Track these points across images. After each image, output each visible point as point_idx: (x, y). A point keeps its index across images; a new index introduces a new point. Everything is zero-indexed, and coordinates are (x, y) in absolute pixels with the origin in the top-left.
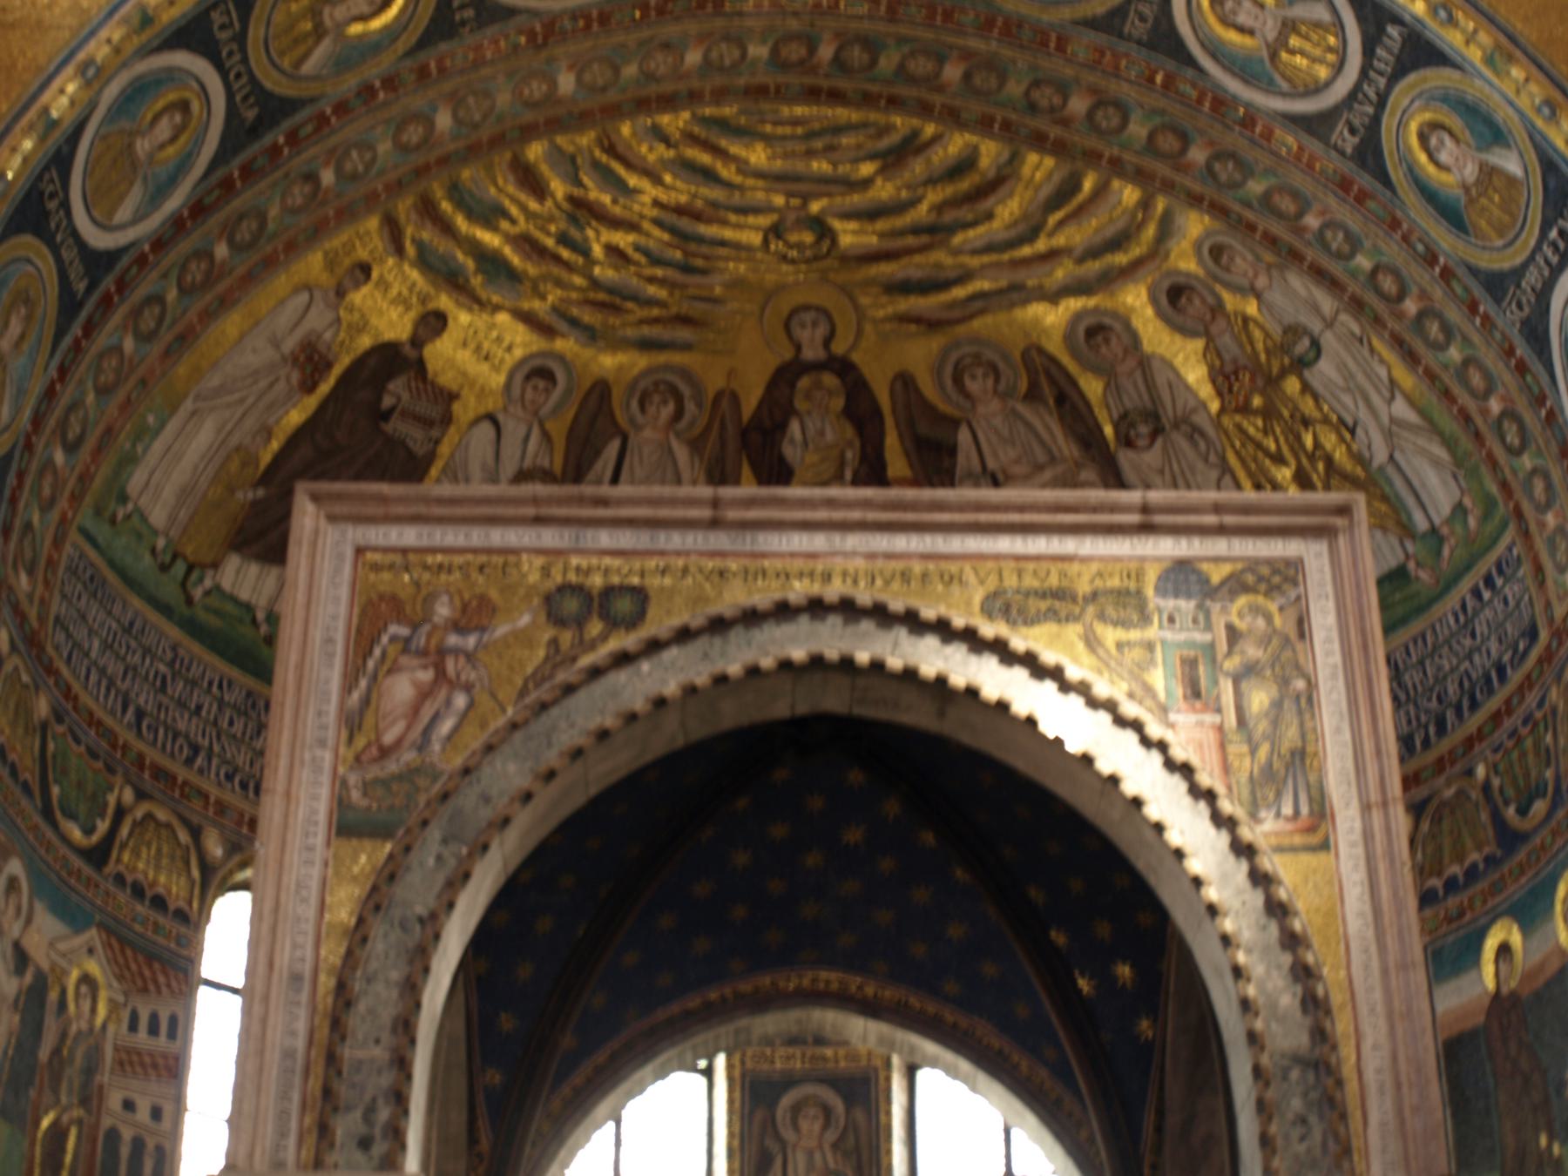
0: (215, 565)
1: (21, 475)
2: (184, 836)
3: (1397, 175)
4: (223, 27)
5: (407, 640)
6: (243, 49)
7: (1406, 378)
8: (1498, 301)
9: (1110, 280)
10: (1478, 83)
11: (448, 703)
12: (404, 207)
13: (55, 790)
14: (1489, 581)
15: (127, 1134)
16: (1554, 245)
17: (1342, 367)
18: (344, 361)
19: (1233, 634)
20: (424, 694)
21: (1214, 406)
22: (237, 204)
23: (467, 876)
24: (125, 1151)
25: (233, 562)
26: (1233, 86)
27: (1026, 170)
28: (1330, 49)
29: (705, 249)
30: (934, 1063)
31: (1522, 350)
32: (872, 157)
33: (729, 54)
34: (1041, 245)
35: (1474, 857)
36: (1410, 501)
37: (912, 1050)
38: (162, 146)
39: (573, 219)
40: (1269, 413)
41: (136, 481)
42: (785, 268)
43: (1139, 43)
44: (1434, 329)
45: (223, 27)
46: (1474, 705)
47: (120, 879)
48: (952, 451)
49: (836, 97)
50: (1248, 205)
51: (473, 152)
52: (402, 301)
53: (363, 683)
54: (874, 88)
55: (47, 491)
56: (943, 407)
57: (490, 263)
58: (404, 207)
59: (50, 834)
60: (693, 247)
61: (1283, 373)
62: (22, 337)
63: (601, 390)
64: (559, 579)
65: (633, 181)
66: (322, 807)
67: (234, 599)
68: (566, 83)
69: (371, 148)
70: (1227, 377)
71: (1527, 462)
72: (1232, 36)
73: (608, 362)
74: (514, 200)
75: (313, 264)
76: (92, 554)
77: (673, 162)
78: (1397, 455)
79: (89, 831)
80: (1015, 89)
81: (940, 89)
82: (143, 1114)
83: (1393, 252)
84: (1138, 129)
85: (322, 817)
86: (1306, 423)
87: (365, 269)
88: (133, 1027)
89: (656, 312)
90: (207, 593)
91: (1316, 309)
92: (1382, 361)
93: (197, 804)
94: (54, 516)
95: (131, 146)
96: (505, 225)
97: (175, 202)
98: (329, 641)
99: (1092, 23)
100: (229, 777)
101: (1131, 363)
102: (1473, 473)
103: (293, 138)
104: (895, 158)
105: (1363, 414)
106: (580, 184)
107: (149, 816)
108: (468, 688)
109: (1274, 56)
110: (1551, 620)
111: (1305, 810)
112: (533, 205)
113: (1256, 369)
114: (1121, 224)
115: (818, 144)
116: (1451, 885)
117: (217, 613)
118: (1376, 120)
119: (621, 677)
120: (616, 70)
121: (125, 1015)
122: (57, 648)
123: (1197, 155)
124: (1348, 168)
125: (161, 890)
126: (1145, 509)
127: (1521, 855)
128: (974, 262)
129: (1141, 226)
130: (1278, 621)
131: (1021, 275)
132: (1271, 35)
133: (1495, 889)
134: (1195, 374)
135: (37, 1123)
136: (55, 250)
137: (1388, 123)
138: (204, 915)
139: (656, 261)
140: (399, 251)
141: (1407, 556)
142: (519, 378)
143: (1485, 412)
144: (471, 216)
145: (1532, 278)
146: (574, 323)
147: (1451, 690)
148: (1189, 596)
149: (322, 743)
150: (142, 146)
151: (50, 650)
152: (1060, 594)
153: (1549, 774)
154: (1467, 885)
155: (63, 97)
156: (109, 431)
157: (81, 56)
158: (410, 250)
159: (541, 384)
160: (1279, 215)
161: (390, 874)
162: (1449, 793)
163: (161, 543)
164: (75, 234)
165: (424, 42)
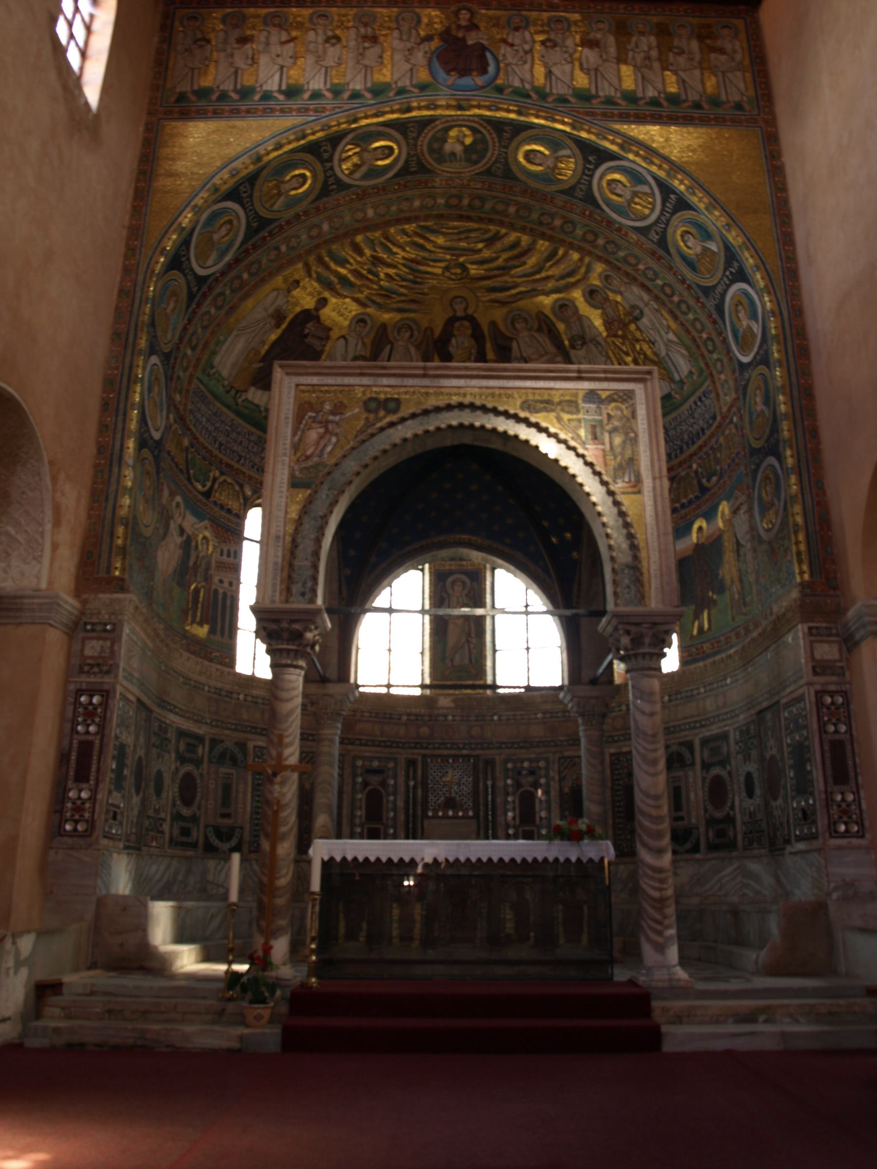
0: (246, 391)
1: (176, 358)
2: (237, 488)
3: (672, 250)
4: (245, 192)
5: (314, 418)
6: (252, 201)
7: (673, 325)
8: (707, 297)
10: (703, 217)
11: (329, 440)
13: (192, 472)
14: (700, 399)
15: (221, 591)
16: (727, 277)
18: (291, 316)
19: (609, 417)
20: (321, 437)
21: (605, 334)
22: (251, 258)
23: (337, 502)
24: (220, 597)
25: (252, 390)
26: (614, 216)
27: (538, 247)
28: (650, 203)
29: (421, 275)
30: (501, 567)
31: (715, 316)
32: (481, 241)
33: (429, 202)
34: (543, 274)
35: (691, 496)
37: (494, 562)
38: (223, 237)
39: (373, 264)
40: (624, 337)
41: (217, 360)
42: (451, 282)
43: (581, 200)
44: (684, 307)
45: (245, 192)
46: (693, 443)
47: (215, 503)
49: (469, 218)
50: (618, 260)
51: (336, 239)
52: (311, 294)
53: (299, 433)
54: (483, 215)
55: (185, 365)
56: (507, 334)
57: (343, 280)
58: (312, 259)
59: (190, 487)
60: (417, 274)
61: (630, 322)
62: (174, 308)
63: (384, 326)
64: (369, 396)
65: (395, 250)
66: (286, 477)
67: (252, 403)
68: (370, 213)
69: (299, 237)
70: (609, 323)
71: (715, 356)
72: (614, 197)
73: (386, 316)
74: (352, 257)
75: (279, 280)
76: (202, 387)
77: (409, 242)
78: (670, 354)
79: (204, 486)
80: (534, 216)
81: (507, 216)
82: (226, 585)
83: (670, 278)
84: (579, 232)
85: (285, 481)
86: (637, 341)
88: (222, 554)
89: (403, 298)
90: (243, 401)
91: (642, 299)
92: (666, 319)
94: (188, 373)
95: (211, 237)
96: (348, 266)
97: (228, 258)
98: (287, 418)
99: (563, 192)
100: (253, 467)
103: (271, 234)
104: (490, 242)
105: (658, 338)
106: (375, 251)
107: (225, 481)
108: (336, 435)
109: (629, 205)
110: (721, 412)
111: (633, 479)
112: (359, 259)
115: (462, 236)
116: (683, 506)
118: (665, 229)
119: (391, 431)
120: (388, 207)
121: (219, 550)
122: (190, 421)
123: (601, 242)
124: (655, 247)
125: (229, 507)
126: (579, 371)
127: (707, 496)
128: (519, 280)
129: (579, 267)
130: (625, 412)
132: (628, 197)
134: (598, 323)
135: (190, 587)
136: (185, 275)
137: (670, 230)
138: (245, 517)
139: (404, 280)
140: (310, 276)
141: (672, 389)
142: (354, 322)
143: (701, 337)
145: (719, 289)
146: (374, 302)
147: (686, 437)
148: (594, 403)
149: (285, 455)
150: (216, 237)
151: (188, 422)
152: (548, 402)
153: (718, 467)
155: (187, 218)
156: (207, 344)
157: (193, 203)
158: (314, 275)
159: (362, 325)
160: (630, 264)
161: (309, 501)
162: (683, 474)
163: (226, 383)
164: (192, 270)
165: (318, 198)
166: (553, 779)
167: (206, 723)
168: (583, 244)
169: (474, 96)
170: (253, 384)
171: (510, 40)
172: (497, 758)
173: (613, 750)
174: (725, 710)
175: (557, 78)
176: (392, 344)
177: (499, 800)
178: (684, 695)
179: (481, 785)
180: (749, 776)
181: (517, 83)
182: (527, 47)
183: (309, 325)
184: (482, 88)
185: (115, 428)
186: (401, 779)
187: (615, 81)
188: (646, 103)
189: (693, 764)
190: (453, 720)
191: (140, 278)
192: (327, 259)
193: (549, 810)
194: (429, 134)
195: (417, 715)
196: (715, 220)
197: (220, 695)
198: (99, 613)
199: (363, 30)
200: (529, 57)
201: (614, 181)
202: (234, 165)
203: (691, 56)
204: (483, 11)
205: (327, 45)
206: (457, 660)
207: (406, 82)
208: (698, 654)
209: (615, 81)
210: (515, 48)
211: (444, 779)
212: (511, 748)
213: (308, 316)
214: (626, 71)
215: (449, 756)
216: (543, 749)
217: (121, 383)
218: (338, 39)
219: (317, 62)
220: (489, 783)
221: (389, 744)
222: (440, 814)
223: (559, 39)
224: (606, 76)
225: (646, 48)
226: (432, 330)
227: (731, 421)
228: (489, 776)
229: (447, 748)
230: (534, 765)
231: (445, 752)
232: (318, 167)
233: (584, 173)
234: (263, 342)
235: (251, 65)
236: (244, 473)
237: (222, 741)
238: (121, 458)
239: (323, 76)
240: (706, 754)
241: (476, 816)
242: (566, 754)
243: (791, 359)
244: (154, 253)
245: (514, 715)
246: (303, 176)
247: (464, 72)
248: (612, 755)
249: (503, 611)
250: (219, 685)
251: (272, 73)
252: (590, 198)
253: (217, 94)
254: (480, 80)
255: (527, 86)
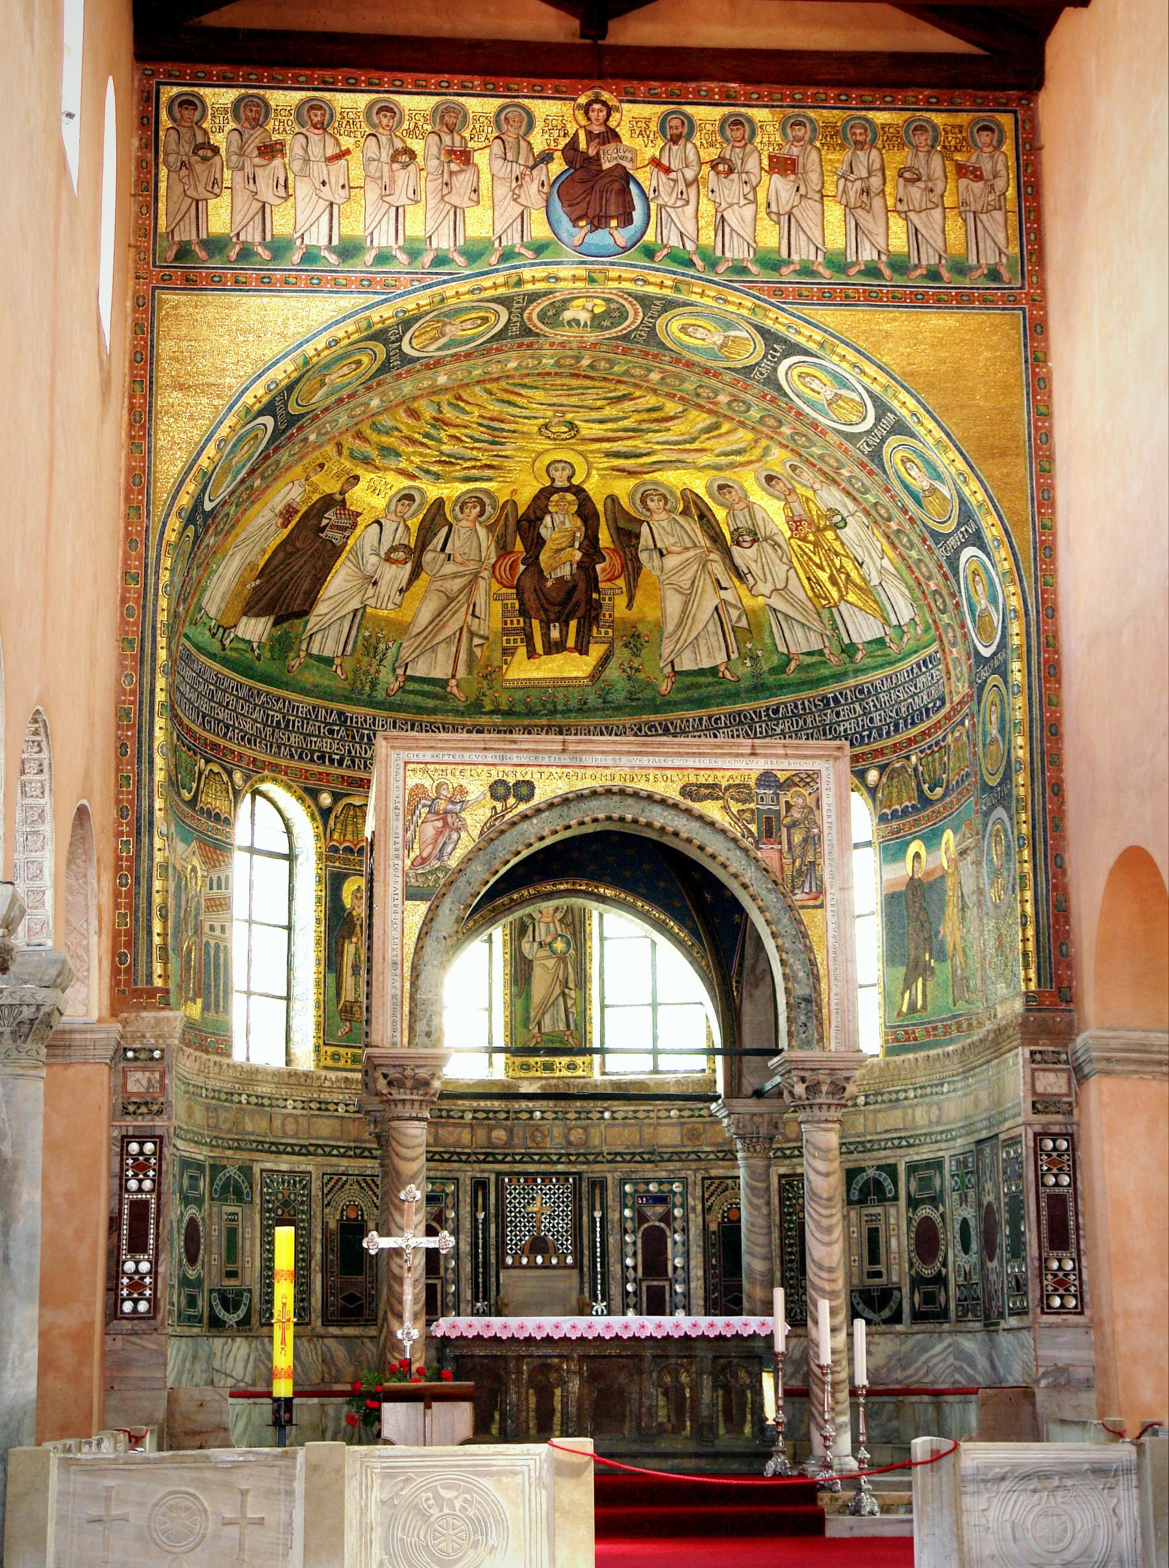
2: (225, 778)
3: (890, 472)
7: (890, 552)
9: (732, 466)
11: (450, 837)
12: (348, 441)
14: (924, 662)
17: (857, 535)
18: (304, 509)
19: (789, 806)
20: (439, 833)
21: (788, 534)
24: (212, 952)
25: (244, 619)
26: (807, 410)
27: (691, 417)
34: (696, 445)
36: (889, 608)
39: (433, 426)
40: (816, 544)
46: (913, 724)
48: (638, 536)
61: (826, 528)
63: (440, 503)
65: (468, 408)
66: (400, 886)
71: (945, 618)
72: (807, 391)
82: (218, 932)
83: (885, 499)
84: (755, 414)
85: (400, 892)
87: (322, 466)
93: (229, 758)
100: (243, 738)
101: (742, 505)
102: (920, 607)
103: (300, 429)
113: (811, 523)
114: (742, 445)
117: (236, 650)
119: (525, 825)
123: (786, 430)
124: (866, 460)
131: (684, 456)
133: (916, 823)
137: (886, 450)
140: (340, 453)
144: (379, 432)
146: (428, 472)
148: (769, 787)
149: (397, 857)
152: (714, 786)
154: (902, 817)
166: (694, 1209)
167: (206, 1144)
168: (759, 427)
169: (612, 264)
170: (245, 614)
171: (665, 162)
172: (609, 1176)
173: (782, 1171)
174: (940, 1128)
175: (732, 230)
176: (451, 526)
177: (612, 1240)
178: (886, 1097)
179: (585, 1218)
180: (965, 1223)
181: (675, 241)
182: (690, 174)
183: (330, 514)
184: (625, 249)
185: (139, 781)
186: (465, 1210)
187: (816, 234)
188: (859, 272)
189: (896, 1198)
190: (542, 1118)
191: (152, 554)
192: (368, 431)
193: (687, 1255)
194: (544, 303)
195: (487, 1112)
196: (950, 462)
197: (219, 1099)
198: (143, 1036)
199: (447, 139)
200: (693, 191)
201: (808, 375)
202: (270, 374)
203: (930, 185)
204: (625, 106)
205: (396, 166)
206: (547, 1026)
207: (512, 239)
208: (908, 1040)
209: (816, 234)
210: (673, 175)
211: (529, 1209)
212: (629, 1162)
213: (328, 502)
214: (834, 212)
215: (538, 1173)
216: (678, 1165)
217: (140, 715)
218: (412, 154)
219: (382, 197)
220: (598, 1214)
221: (446, 1156)
222: (524, 1261)
223: (736, 156)
224: (804, 225)
225: (864, 174)
226: (515, 503)
227: (962, 723)
228: (598, 1206)
229: (533, 1162)
230: (665, 1188)
231: (531, 1168)
232: (380, 350)
233: (765, 356)
234: (264, 551)
235: (286, 199)
236: (233, 752)
237: (225, 1167)
238: (151, 824)
239: (393, 221)
240: (913, 1186)
241: (578, 1265)
242: (714, 1173)
243: (1035, 684)
244: (168, 515)
245: (635, 1112)
246: (359, 363)
247: (598, 222)
248: (781, 1176)
249: (655, 1038)
250: (218, 1085)
251: (316, 214)
252: (772, 381)
253: (237, 248)
254: (623, 236)
255: (690, 246)
